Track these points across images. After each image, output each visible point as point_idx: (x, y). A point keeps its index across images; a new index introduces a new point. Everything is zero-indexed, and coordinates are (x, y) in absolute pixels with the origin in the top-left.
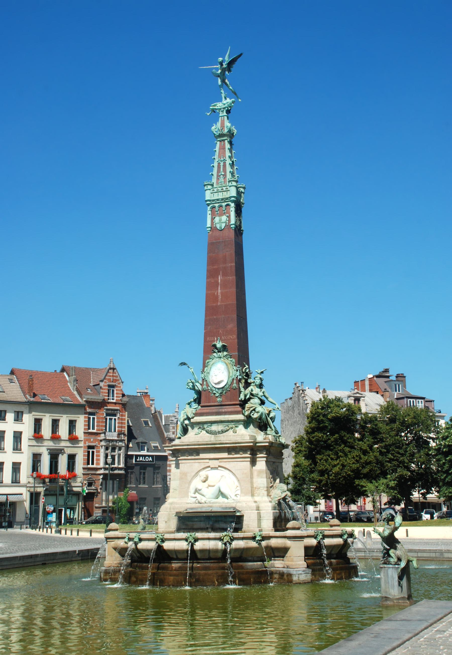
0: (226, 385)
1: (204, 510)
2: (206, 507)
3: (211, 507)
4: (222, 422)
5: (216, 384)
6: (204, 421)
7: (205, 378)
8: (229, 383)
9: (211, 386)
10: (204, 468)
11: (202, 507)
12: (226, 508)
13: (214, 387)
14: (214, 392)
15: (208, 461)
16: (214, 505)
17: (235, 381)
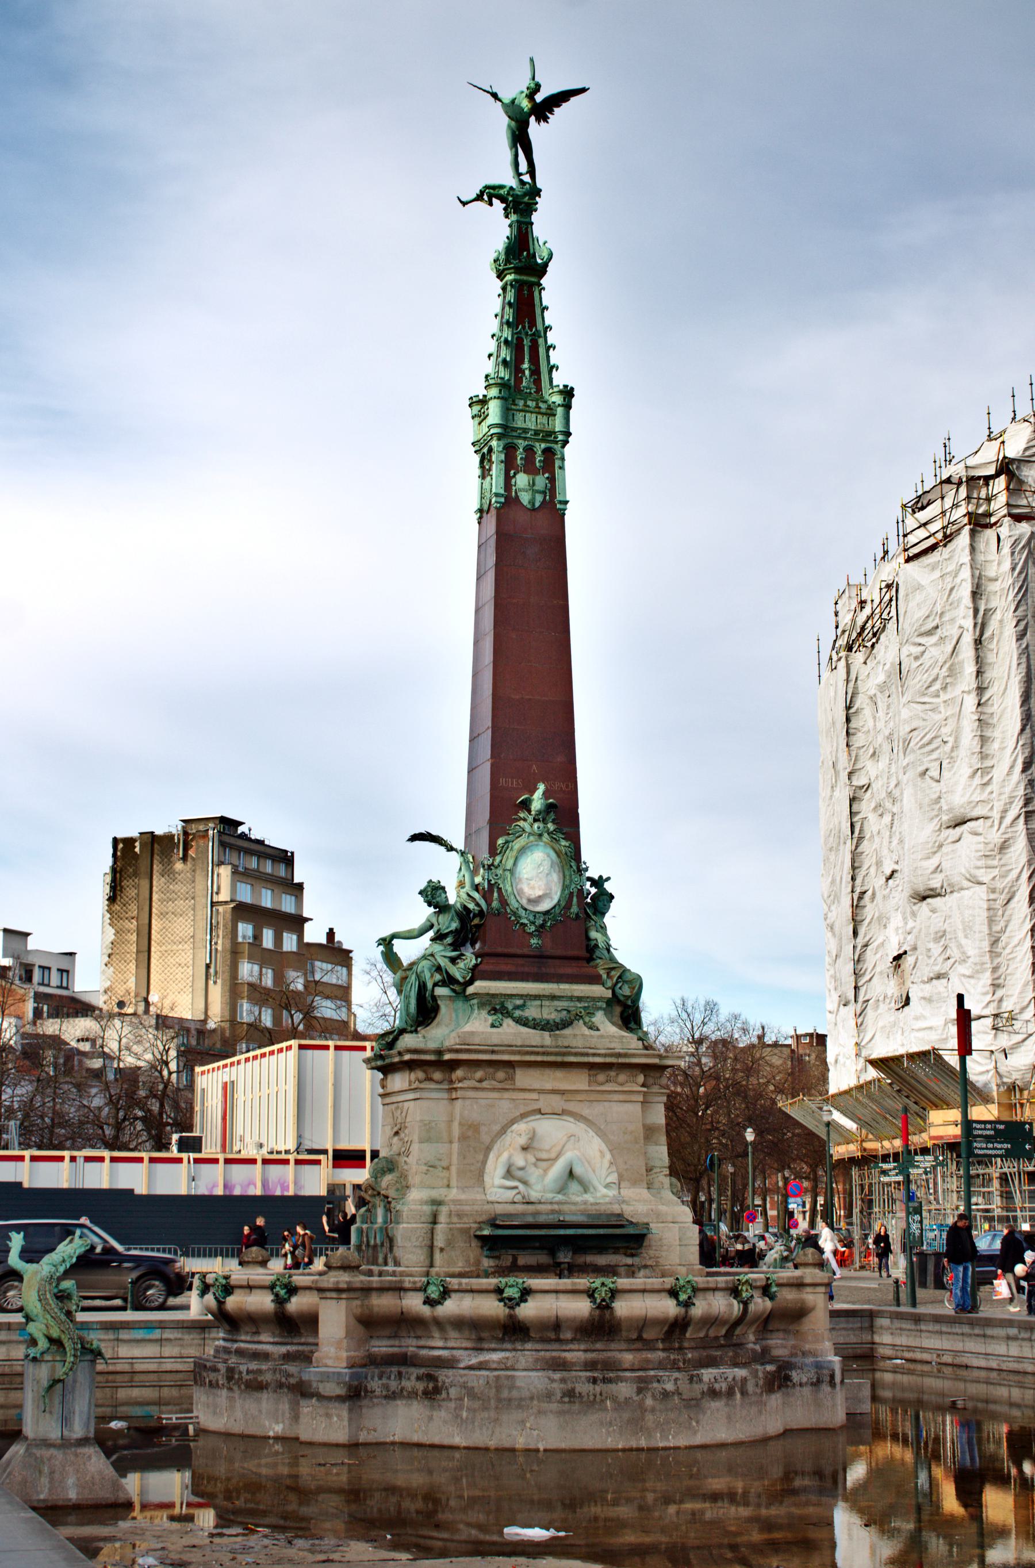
0: (554, 907)
1: (542, 1219)
2: (547, 1214)
3: (559, 1212)
4: (553, 997)
5: (530, 901)
6: (509, 992)
7: (499, 882)
8: (563, 904)
9: (514, 904)
10: (523, 1116)
11: (537, 1213)
12: (599, 1215)
13: (526, 910)
14: (525, 921)
15: (535, 1096)
16: (566, 1208)
17: (575, 899)
